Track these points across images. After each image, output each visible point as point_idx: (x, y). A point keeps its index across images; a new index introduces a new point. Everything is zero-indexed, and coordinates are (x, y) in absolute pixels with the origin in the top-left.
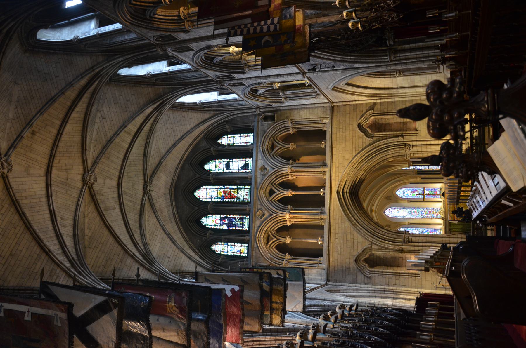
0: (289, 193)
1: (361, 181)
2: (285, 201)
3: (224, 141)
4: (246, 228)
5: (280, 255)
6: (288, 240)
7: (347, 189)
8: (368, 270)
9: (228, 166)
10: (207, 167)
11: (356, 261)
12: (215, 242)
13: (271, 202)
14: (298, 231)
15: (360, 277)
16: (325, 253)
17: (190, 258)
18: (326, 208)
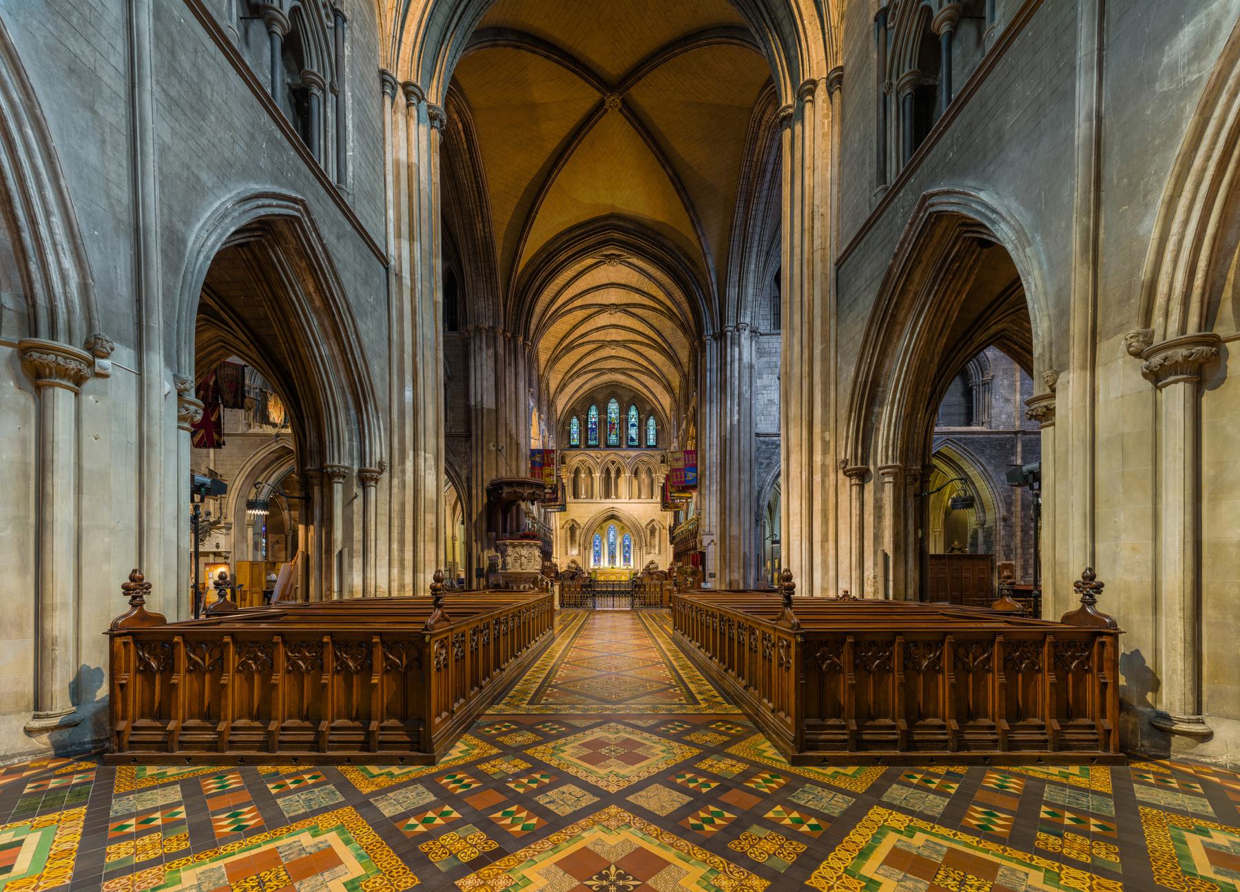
0: (613, 475)
1: (620, 521)
2: (608, 471)
3: (651, 422)
4: (591, 443)
5: (573, 470)
6: (583, 475)
7: (615, 513)
8: (568, 526)
9: (633, 425)
10: (633, 408)
11: (573, 520)
12: (579, 419)
13: (607, 463)
14: (589, 480)
15: (563, 522)
16: (576, 500)
17: (566, 405)
18: (603, 500)
